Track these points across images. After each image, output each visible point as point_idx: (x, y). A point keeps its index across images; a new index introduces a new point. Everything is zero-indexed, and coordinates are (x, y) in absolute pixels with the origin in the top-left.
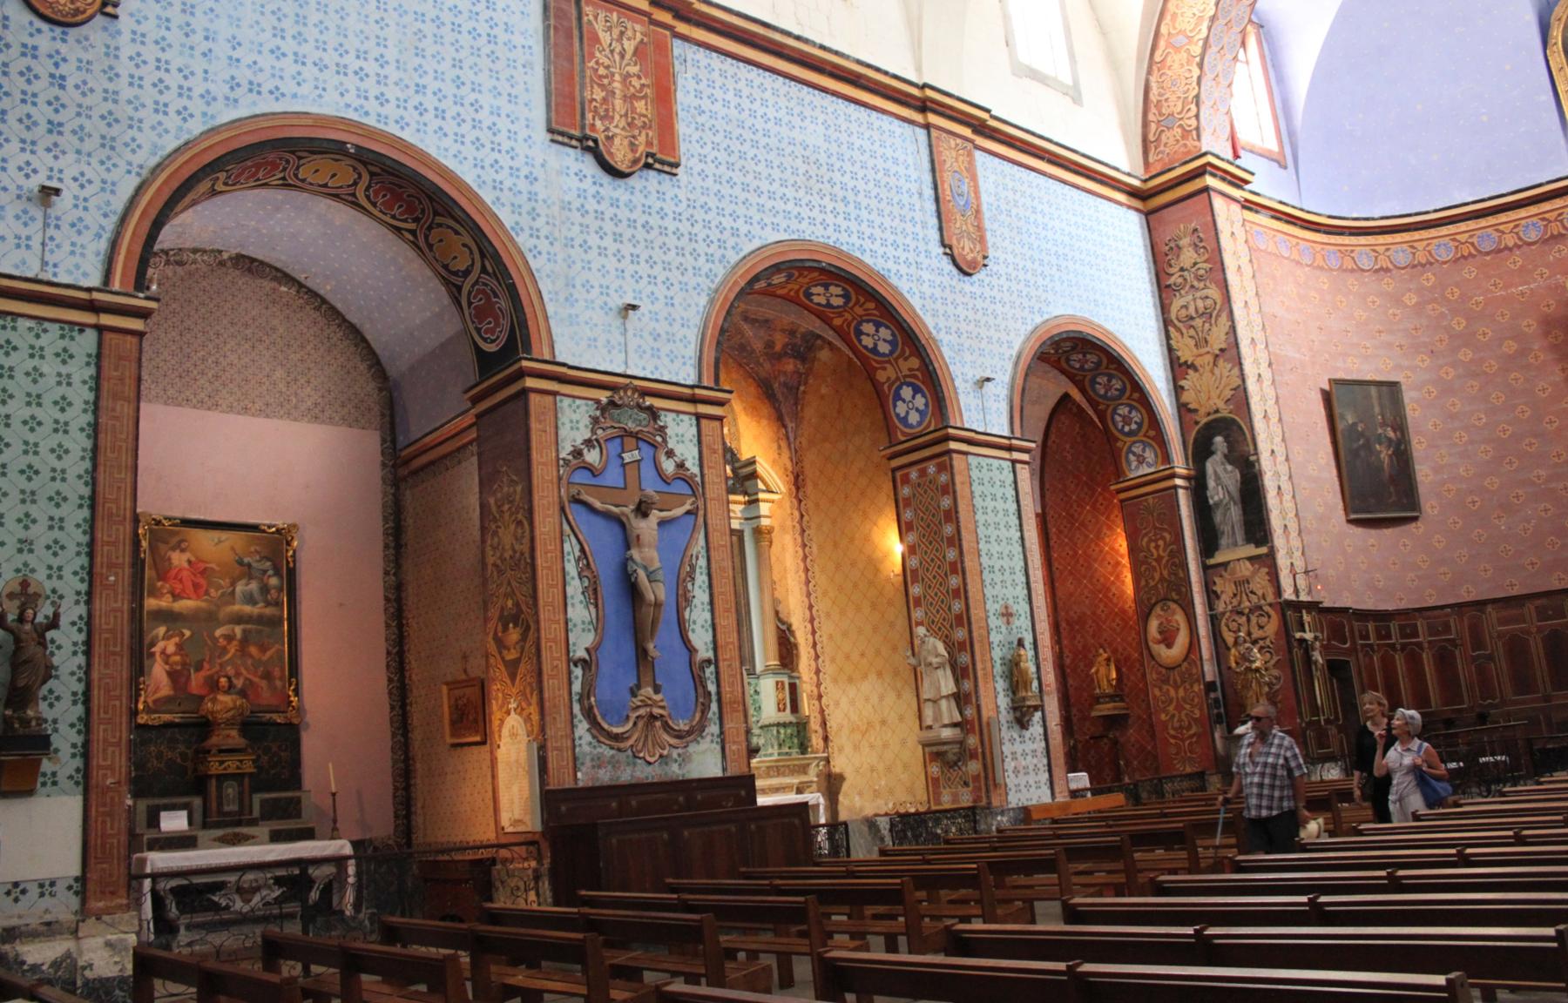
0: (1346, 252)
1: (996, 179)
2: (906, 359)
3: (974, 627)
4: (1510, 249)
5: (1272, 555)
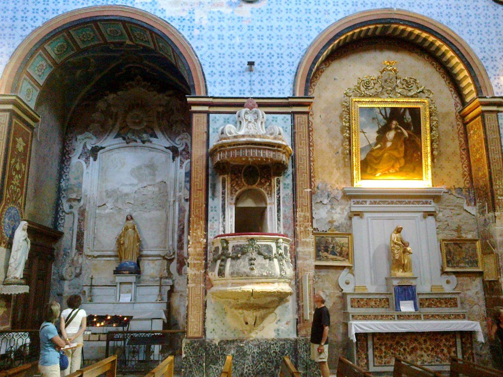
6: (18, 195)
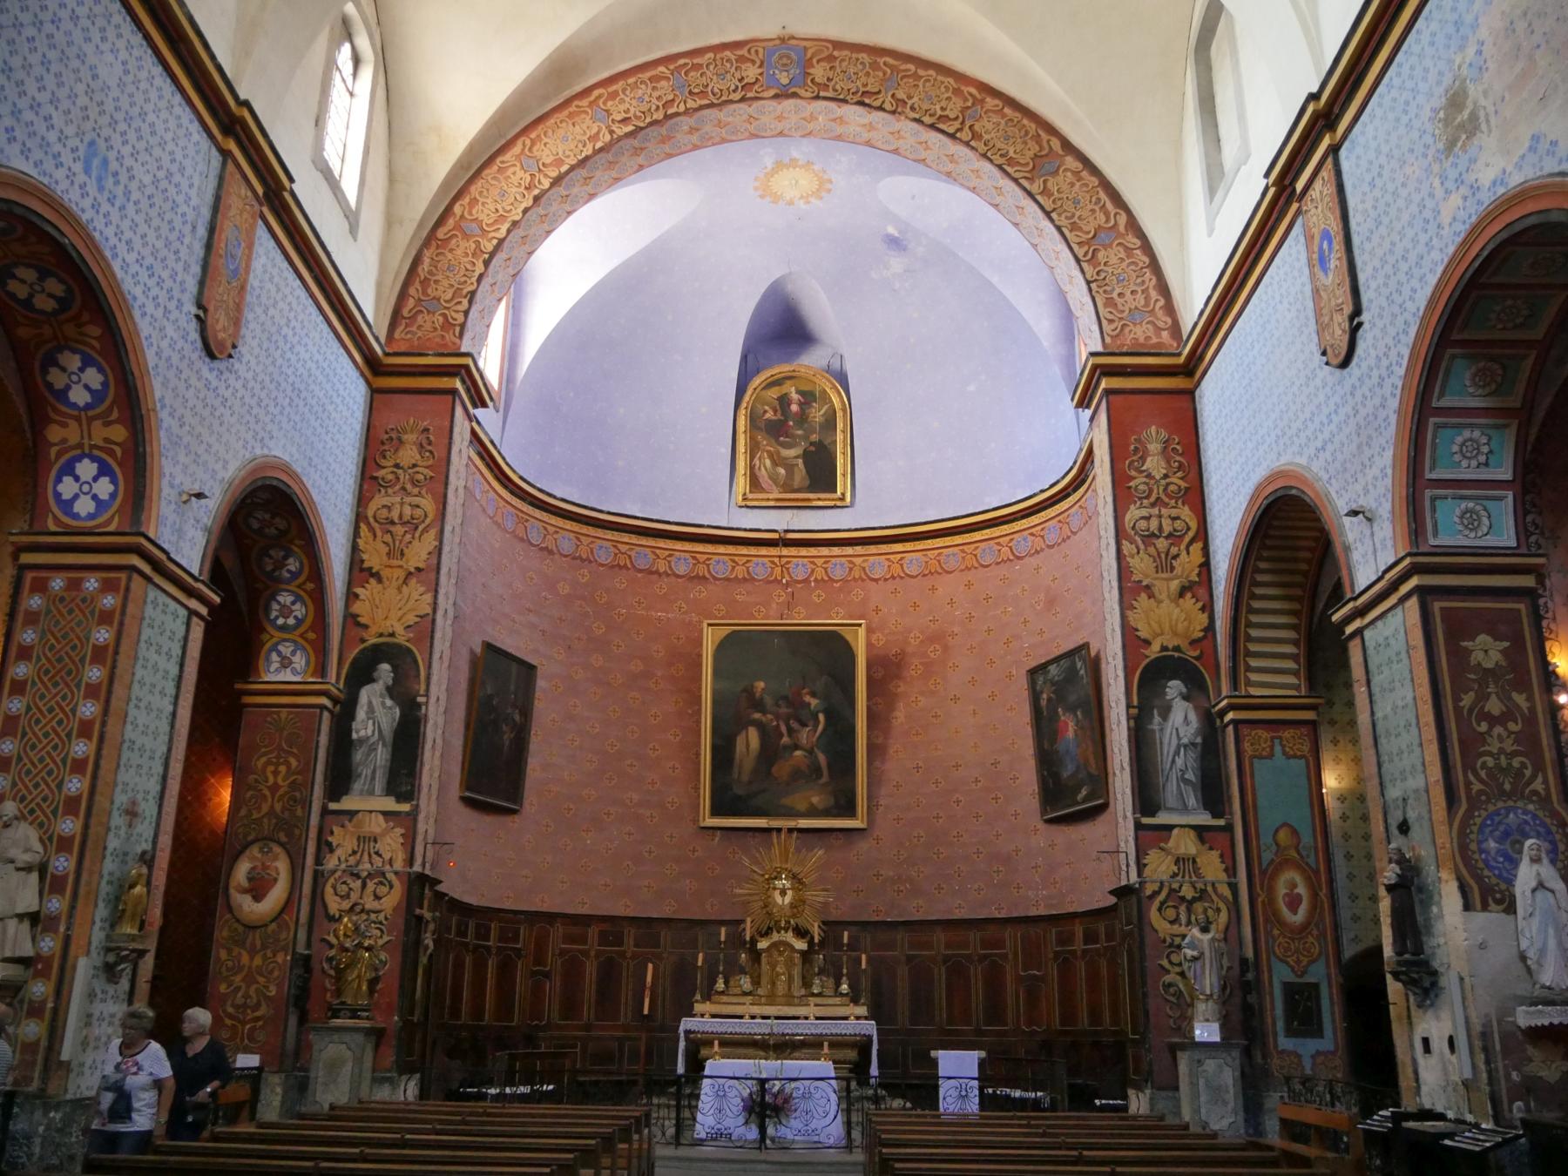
0: (523, 520)
1: (268, 263)
2: (107, 424)
3: (93, 821)
4: (660, 575)
5: (413, 815)
6: (1519, 773)
